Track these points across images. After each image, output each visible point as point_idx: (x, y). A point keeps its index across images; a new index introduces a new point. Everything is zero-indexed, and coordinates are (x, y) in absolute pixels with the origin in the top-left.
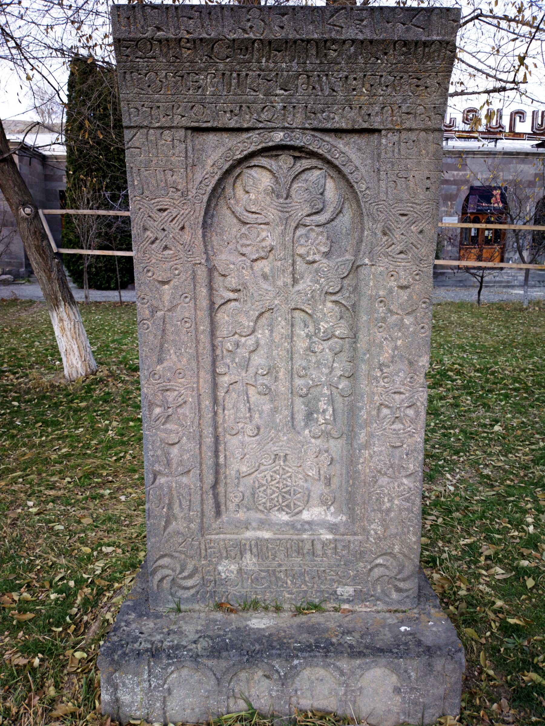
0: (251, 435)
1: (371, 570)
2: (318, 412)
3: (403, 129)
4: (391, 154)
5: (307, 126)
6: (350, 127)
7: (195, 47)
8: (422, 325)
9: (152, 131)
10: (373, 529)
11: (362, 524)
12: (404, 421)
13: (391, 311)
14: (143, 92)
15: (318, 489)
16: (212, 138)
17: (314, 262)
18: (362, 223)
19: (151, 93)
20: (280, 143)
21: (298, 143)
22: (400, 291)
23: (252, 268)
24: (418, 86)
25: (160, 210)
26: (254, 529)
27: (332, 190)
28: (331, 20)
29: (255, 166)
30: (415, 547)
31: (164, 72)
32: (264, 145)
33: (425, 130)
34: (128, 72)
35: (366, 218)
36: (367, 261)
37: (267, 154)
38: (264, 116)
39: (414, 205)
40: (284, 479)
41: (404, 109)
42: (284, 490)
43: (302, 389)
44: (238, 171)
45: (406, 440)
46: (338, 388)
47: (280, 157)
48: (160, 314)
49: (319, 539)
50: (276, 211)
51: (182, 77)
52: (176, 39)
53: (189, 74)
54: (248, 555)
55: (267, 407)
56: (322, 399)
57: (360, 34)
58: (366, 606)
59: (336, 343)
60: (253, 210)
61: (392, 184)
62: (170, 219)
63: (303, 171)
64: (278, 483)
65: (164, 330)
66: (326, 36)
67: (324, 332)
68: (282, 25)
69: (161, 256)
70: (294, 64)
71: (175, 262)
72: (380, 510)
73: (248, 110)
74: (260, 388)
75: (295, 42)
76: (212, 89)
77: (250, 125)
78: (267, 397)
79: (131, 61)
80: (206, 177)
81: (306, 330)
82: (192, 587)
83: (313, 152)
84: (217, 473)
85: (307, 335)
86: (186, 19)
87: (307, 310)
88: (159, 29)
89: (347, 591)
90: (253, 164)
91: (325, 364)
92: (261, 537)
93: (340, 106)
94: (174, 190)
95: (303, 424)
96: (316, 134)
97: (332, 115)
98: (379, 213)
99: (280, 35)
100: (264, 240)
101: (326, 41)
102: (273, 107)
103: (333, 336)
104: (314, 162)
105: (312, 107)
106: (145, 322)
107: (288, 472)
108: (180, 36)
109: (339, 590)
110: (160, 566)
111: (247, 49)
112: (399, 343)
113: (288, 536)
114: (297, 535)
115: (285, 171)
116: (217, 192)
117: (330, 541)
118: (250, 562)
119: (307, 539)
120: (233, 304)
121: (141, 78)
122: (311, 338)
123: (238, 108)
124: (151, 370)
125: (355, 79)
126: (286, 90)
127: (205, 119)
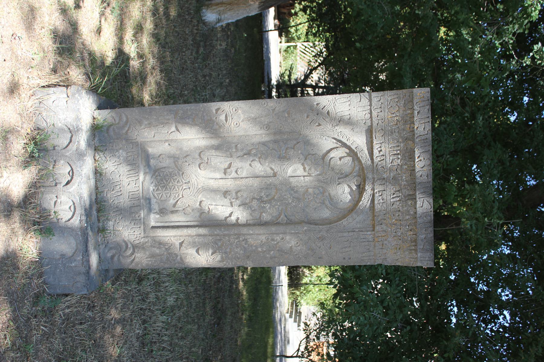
4: (362, 237)
5: (376, 191)
35: (329, 226)
49: (141, 209)
51: (397, 124)
52: (414, 121)
66: (418, 199)
75: (415, 183)
81: (264, 196)
85: (262, 197)
101: (415, 199)
104: (357, 196)
125: (399, 215)
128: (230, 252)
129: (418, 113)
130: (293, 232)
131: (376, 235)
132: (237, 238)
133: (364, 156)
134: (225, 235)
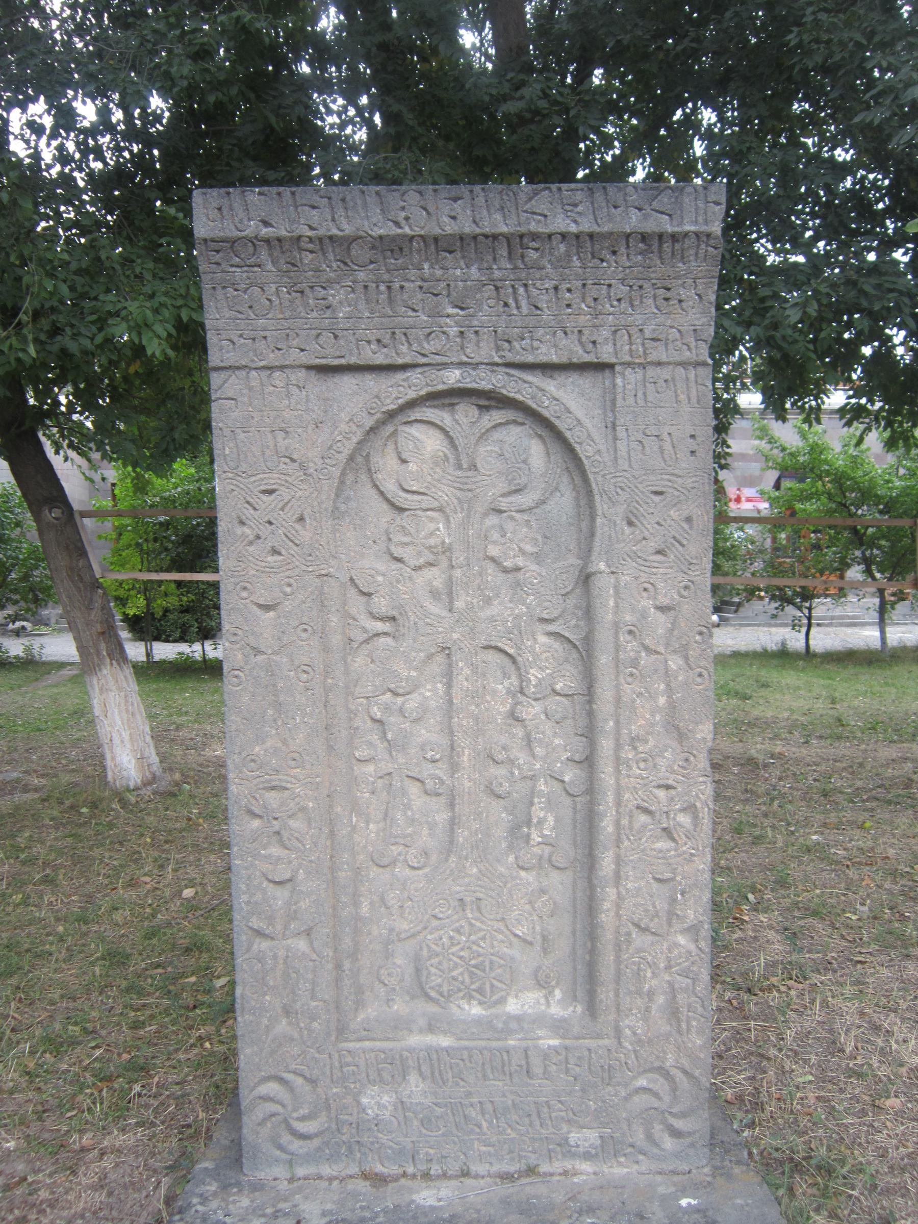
0: (416, 865)
1: (627, 1099)
2: (529, 823)
3: (648, 363)
4: (631, 401)
5: (497, 359)
6: (564, 360)
7: (322, 249)
8: (699, 670)
9: (254, 373)
10: (629, 1027)
12: (675, 836)
13: (646, 648)
14: (240, 316)
16: (348, 382)
17: (518, 569)
18: (591, 505)
19: (253, 317)
20: (456, 386)
21: (485, 385)
22: (659, 614)
24: (667, 299)
25: (265, 492)
26: (421, 1031)
29: (416, 421)
30: (702, 1056)
31: (273, 286)
32: (430, 389)
33: (684, 364)
35: (597, 498)
36: (602, 566)
37: (436, 403)
40: (474, 943)
41: (648, 334)
42: (473, 962)
43: (501, 784)
44: (390, 429)
45: (680, 869)
46: (563, 782)
47: (457, 407)
49: (536, 1047)
50: (452, 490)
52: (291, 238)
53: (312, 287)
54: (413, 1078)
57: (573, 225)
58: (620, 1164)
59: (558, 704)
60: (414, 488)
61: (635, 445)
63: (494, 427)
64: (462, 949)
66: (523, 230)
67: (535, 686)
68: (453, 214)
69: (263, 564)
70: (474, 270)
71: (287, 573)
72: (639, 992)
73: (403, 338)
75: (475, 238)
76: (348, 309)
77: (407, 360)
79: (223, 271)
80: (339, 438)
81: (506, 683)
82: (316, 1135)
83: (508, 398)
86: (307, 208)
87: (507, 649)
89: (585, 1137)
90: (413, 418)
91: (540, 739)
92: (434, 1044)
93: (547, 330)
94: (288, 460)
95: (504, 845)
97: (536, 344)
98: (619, 490)
99: (450, 228)
101: (521, 236)
102: (444, 333)
104: (510, 414)
105: (504, 333)
106: (236, 672)
107: (481, 930)
109: (574, 1137)
110: (260, 1098)
111: (401, 249)
113: (483, 1043)
114: (498, 1040)
118: (416, 1088)
119: (514, 1047)
120: (382, 640)
121: (238, 296)
122: (514, 696)
123: (388, 336)
124: (244, 754)
125: (569, 290)
126: (462, 309)
127: (338, 353)
128: (668, 787)
129: (266, 224)
130: (612, 603)
131: (627, 358)
132: (630, 768)
133: (394, 392)
134: (618, 803)
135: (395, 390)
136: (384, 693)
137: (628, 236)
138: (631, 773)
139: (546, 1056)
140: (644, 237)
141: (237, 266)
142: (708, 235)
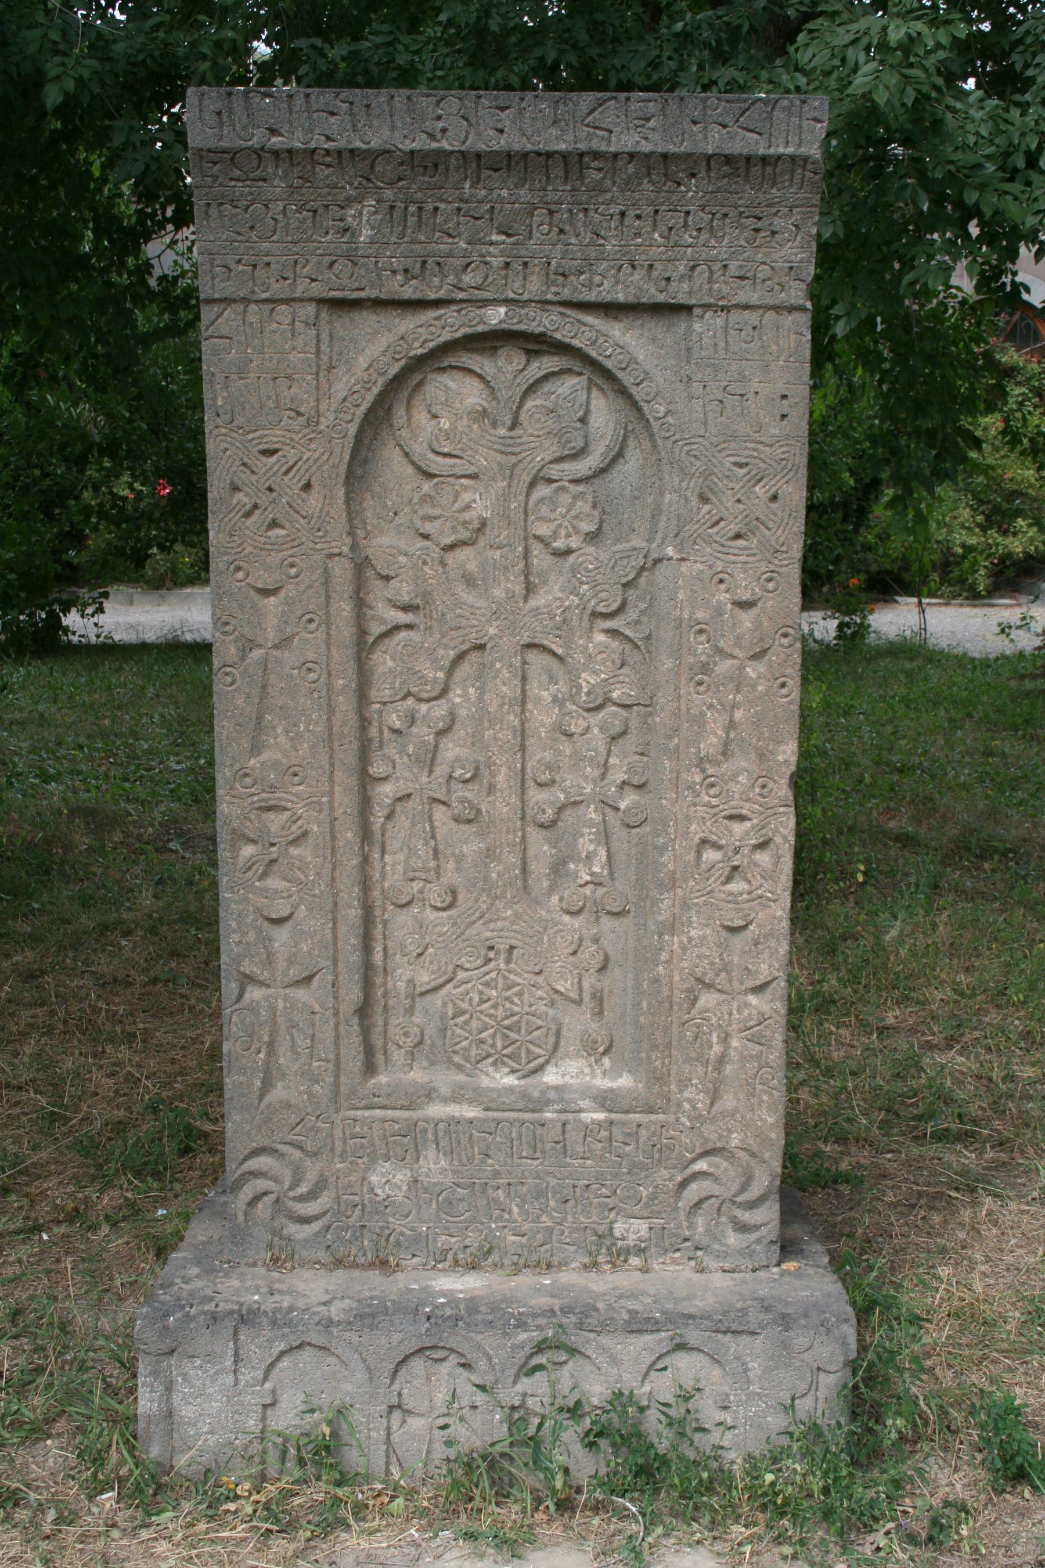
0: (439, 905)
1: (683, 1184)
2: (574, 857)
3: (737, 306)
5: (549, 297)
6: (631, 299)
8: (783, 679)
9: (253, 307)
11: (666, 1089)
12: (749, 876)
13: (720, 651)
14: (240, 238)
15: (577, 1022)
17: (569, 552)
19: (255, 239)
21: (534, 327)
22: (736, 610)
23: (443, 563)
24: (757, 230)
27: (604, 416)
28: (591, 118)
30: (773, 1136)
33: (776, 308)
34: (214, 204)
35: (666, 469)
36: (670, 551)
38: (467, 279)
39: (760, 447)
40: (507, 999)
42: (506, 1022)
43: (544, 811)
44: (417, 377)
46: (617, 809)
47: (500, 352)
48: (256, 654)
50: (491, 452)
51: (315, 212)
52: (305, 150)
53: (327, 206)
54: (431, 1153)
55: (472, 848)
56: (586, 830)
57: (643, 142)
59: (614, 715)
62: (284, 469)
64: (495, 1006)
65: (264, 687)
66: (582, 146)
67: (588, 694)
68: (500, 126)
69: (263, 540)
71: (291, 552)
73: (437, 268)
74: (457, 808)
75: (525, 155)
77: (442, 294)
78: (473, 828)
79: (220, 185)
80: (355, 388)
81: (553, 688)
82: (316, 1218)
84: (367, 984)
85: (555, 698)
87: (554, 647)
88: (273, 132)
90: (446, 364)
91: (592, 759)
92: (457, 1114)
93: (612, 263)
94: (293, 414)
96: (569, 312)
98: (692, 459)
100: (467, 507)
101: (582, 155)
102: (486, 263)
103: (607, 700)
105: (559, 265)
106: (228, 669)
108: (313, 145)
109: (619, 1228)
110: (251, 1173)
111: (436, 166)
112: (738, 714)
114: (533, 1111)
115: (510, 377)
116: (378, 418)
117: (599, 1124)
119: (552, 1120)
120: (403, 634)
122: (562, 705)
123: (418, 265)
124: (237, 767)
125: (639, 217)
126: (509, 235)
135: (423, 331)
136: (404, 698)
137: (709, 158)
138: (698, 800)
139: (588, 1131)
140: (728, 159)
141: (238, 180)
142: (806, 159)
